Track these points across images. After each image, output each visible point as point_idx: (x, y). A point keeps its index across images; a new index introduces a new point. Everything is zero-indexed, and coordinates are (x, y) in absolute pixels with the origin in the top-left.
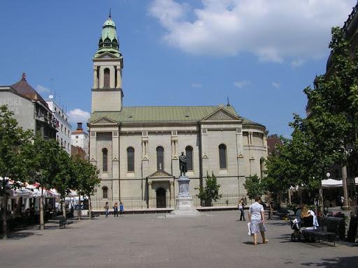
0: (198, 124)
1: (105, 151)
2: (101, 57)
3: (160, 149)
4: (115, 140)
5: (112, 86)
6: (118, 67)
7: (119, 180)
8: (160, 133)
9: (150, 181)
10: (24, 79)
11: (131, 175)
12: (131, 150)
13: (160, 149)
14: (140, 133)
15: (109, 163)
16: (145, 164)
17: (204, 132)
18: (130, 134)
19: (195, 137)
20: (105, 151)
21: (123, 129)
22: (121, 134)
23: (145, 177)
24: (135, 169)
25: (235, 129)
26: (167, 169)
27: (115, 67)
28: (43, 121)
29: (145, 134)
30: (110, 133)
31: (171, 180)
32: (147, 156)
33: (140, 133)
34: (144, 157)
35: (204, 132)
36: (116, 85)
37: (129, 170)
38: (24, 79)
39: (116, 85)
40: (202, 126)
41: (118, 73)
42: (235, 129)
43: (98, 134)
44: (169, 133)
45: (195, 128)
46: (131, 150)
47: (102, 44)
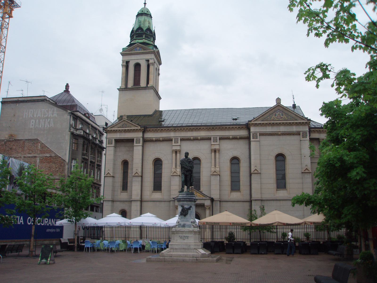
0: (247, 126)
1: (125, 164)
2: (131, 50)
4: (138, 149)
5: (143, 83)
6: (151, 61)
7: (141, 201)
8: (196, 139)
10: (67, 90)
11: (157, 196)
12: (158, 163)
14: (169, 140)
15: (129, 179)
17: (255, 137)
18: (157, 140)
19: (242, 145)
20: (125, 164)
21: (149, 135)
22: (145, 141)
25: (298, 134)
27: (148, 61)
28: (82, 134)
29: (176, 142)
30: (131, 141)
33: (170, 140)
35: (255, 137)
36: (148, 83)
37: (154, 190)
38: (67, 90)
39: (148, 83)
40: (253, 129)
41: (151, 68)
42: (298, 134)
43: (117, 141)
44: (209, 139)
45: (243, 133)
46: (158, 163)
47: (133, 35)
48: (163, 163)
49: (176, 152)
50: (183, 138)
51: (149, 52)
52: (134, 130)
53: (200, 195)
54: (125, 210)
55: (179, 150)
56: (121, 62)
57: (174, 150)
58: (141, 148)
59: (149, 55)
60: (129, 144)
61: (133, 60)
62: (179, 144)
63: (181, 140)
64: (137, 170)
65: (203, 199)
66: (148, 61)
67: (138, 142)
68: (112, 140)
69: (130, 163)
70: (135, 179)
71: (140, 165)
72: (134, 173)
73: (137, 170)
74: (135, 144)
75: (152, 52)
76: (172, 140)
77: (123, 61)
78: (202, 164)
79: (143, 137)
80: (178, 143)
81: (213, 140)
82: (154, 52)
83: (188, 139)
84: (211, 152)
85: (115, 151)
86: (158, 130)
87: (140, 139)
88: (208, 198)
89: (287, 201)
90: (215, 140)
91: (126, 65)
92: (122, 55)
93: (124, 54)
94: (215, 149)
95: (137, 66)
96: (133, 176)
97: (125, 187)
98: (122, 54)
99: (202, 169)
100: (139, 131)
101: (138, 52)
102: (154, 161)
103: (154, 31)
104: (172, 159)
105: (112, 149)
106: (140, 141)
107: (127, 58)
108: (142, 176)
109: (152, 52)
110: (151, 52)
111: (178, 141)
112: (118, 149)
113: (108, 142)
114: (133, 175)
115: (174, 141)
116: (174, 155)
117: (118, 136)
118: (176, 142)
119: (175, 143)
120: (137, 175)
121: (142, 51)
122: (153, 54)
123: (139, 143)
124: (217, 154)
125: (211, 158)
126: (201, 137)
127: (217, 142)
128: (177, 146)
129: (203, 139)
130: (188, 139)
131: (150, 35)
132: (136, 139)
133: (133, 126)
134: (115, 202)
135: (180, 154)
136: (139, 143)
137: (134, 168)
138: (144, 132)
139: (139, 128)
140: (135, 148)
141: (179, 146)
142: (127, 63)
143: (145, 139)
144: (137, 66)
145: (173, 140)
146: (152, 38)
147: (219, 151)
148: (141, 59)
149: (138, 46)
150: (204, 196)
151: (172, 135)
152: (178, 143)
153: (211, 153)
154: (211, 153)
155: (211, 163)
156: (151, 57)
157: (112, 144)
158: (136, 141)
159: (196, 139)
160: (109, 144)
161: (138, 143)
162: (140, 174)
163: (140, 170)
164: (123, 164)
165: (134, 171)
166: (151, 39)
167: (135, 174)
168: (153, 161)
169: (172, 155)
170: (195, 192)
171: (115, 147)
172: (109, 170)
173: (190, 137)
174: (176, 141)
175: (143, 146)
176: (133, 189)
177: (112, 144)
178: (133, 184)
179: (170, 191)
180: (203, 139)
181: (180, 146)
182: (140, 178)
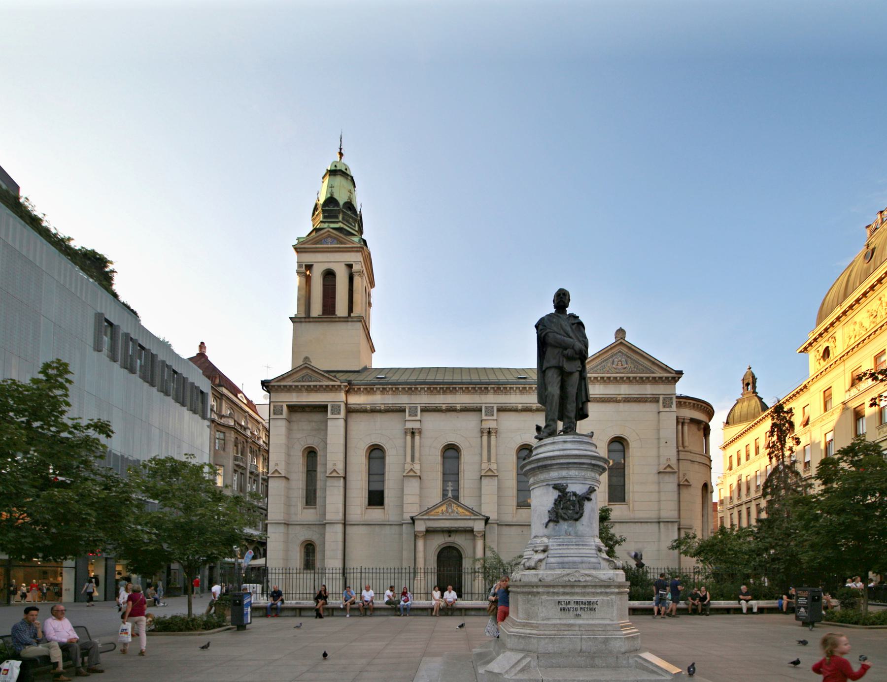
3: (451, 451)
4: (335, 426)
6: (356, 268)
8: (451, 410)
9: (421, 527)
12: (376, 452)
13: (451, 451)
16: (412, 487)
23: (407, 517)
24: (386, 501)
26: (466, 498)
27: (350, 266)
29: (413, 412)
30: (323, 408)
31: (479, 526)
32: (417, 467)
34: (408, 467)
41: (357, 280)
43: (293, 408)
46: (376, 452)
48: (387, 454)
49: (413, 433)
50: (426, 407)
51: (352, 248)
52: (327, 386)
53: (464, 511)
54: (311, 541)
55: (419, 429)
56: (295, 267)
57: (410, 429)
58: (341, 423)
59: (353, 254)
60: (317, 417)
61: (322, 262)
62: (418, 418)
63: (422, 410)
64: (335, 465)
65: (470, 519)
66: (350, 266)
67: (336, 409)
68: (282, 406)
69: (319, 453)
70: (329, 483)
71: (341, 456)
72: (328, 472)
73: (335, 465)
74: (330, 415)
75: (358, 249)
76: (404, 411)
77: (300, 266)
78: (462, 456)
79: (346, 404)
80: (416, 416)
81: (486, 411)
82: (360, 249)
83: (437, 410)
84: (480, 435)
85: (289, 430)
86: (377, 388)
87: (339, 406)
88: (481, 517)
89: (628, 524)
90: (489, 411)
91: (305, 271)
92: (297, 252)
93: (300, 248)
94: (489, 429)
95: (329, 275)
96: (327, 477)
97: (311, 498)
98: (298, 249)
99: (463, 467)
100: (337, 389)
101: (329, 246)
102: (369, 451)
103: (360, 212)
104: (405, 447)
105: (283, 423)
106: (340, 410)
107: (309, 258)
108: (345, 478)
109: (357, 247)
110: (356, 249)
111: (417, 412)
112: (295, 426)
113: (274, 410)
114: (327, 475)
115: (409, 412)
116: (409, 438)
117: (295, 398)
118: (413, 412)
119: (410, 415)
120: (334, 474)
121: (338, 246)
122: (361, 253)
123: (339, 413)
124: (493, 438)
125: (481, 447)
126: (463, 405)
127: (493, 415)
128: (414, 422)
129: (465, 410)
130: (437, 410)
131: (352, 218)
132: (332, 406)
133: (324, 379)
134: (291, 527)
135: (420, 436)
136: (339, 413)
137: (328, 462)
138: (347, 392)
139: (339, 383)
140: (329, 423)
141: (419, 423)
142: (309, 267)
143: (351, 408)
144: (329, 275)
145: (407, 411)
146: (357, 225)
147: (496, 432)
148: (337, 262)
149: (329, 236)
150: (473, 513)
151: (403, 400)
152: (416, 416)
153: (481, 437)
154: (481, 437)
155: (481, 455)
156: (355, 258)
157: (281, 414)
158: (332, 410)
159: (451, 410)
160: (274, 414)
161: (335, 414)
162: (342, 474)
163: (340, 467)
164: (306, 455)
165: (330, 467)
166: (355, 226)
167: (331, 473)
168: (366, 451)
169: (406, 438)
170: (455, 506)
171: (289, 421)
172: (276, 464)
173: (441, 405)
174: (413, 412)
175: (346, 421)
176: (327, 502)
177: (281, 414)
178: (327, 492)
179: (401, 506)
180: (465, 410)
181: (420, 421)
182: (342, 480)
